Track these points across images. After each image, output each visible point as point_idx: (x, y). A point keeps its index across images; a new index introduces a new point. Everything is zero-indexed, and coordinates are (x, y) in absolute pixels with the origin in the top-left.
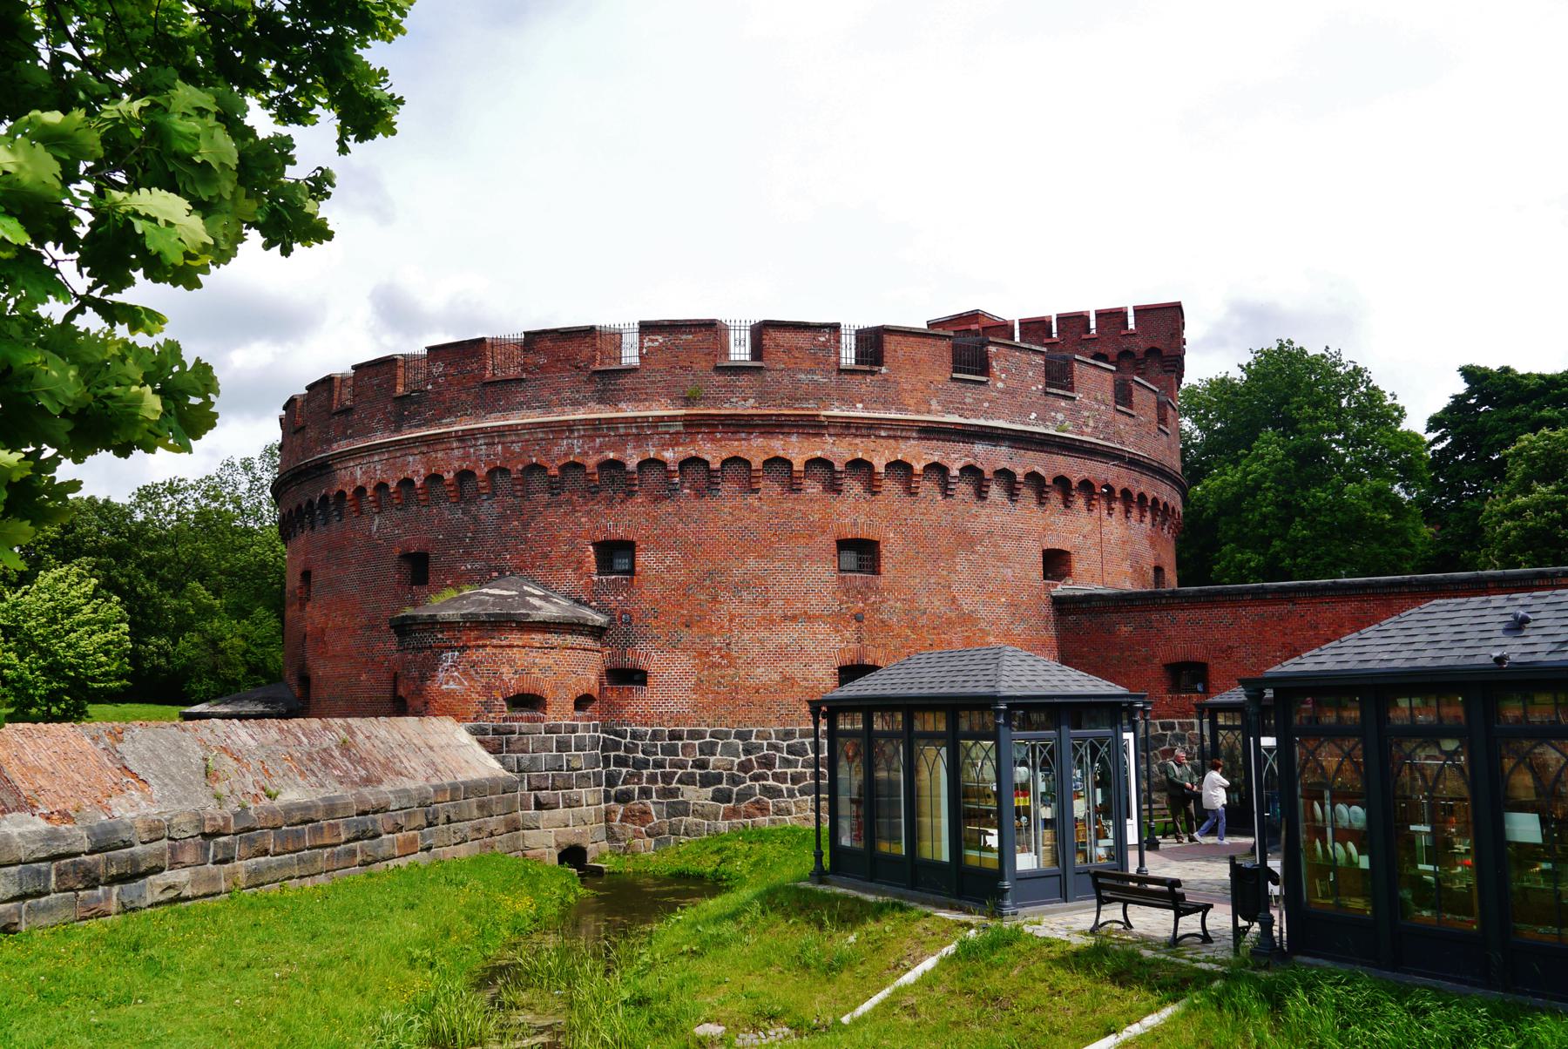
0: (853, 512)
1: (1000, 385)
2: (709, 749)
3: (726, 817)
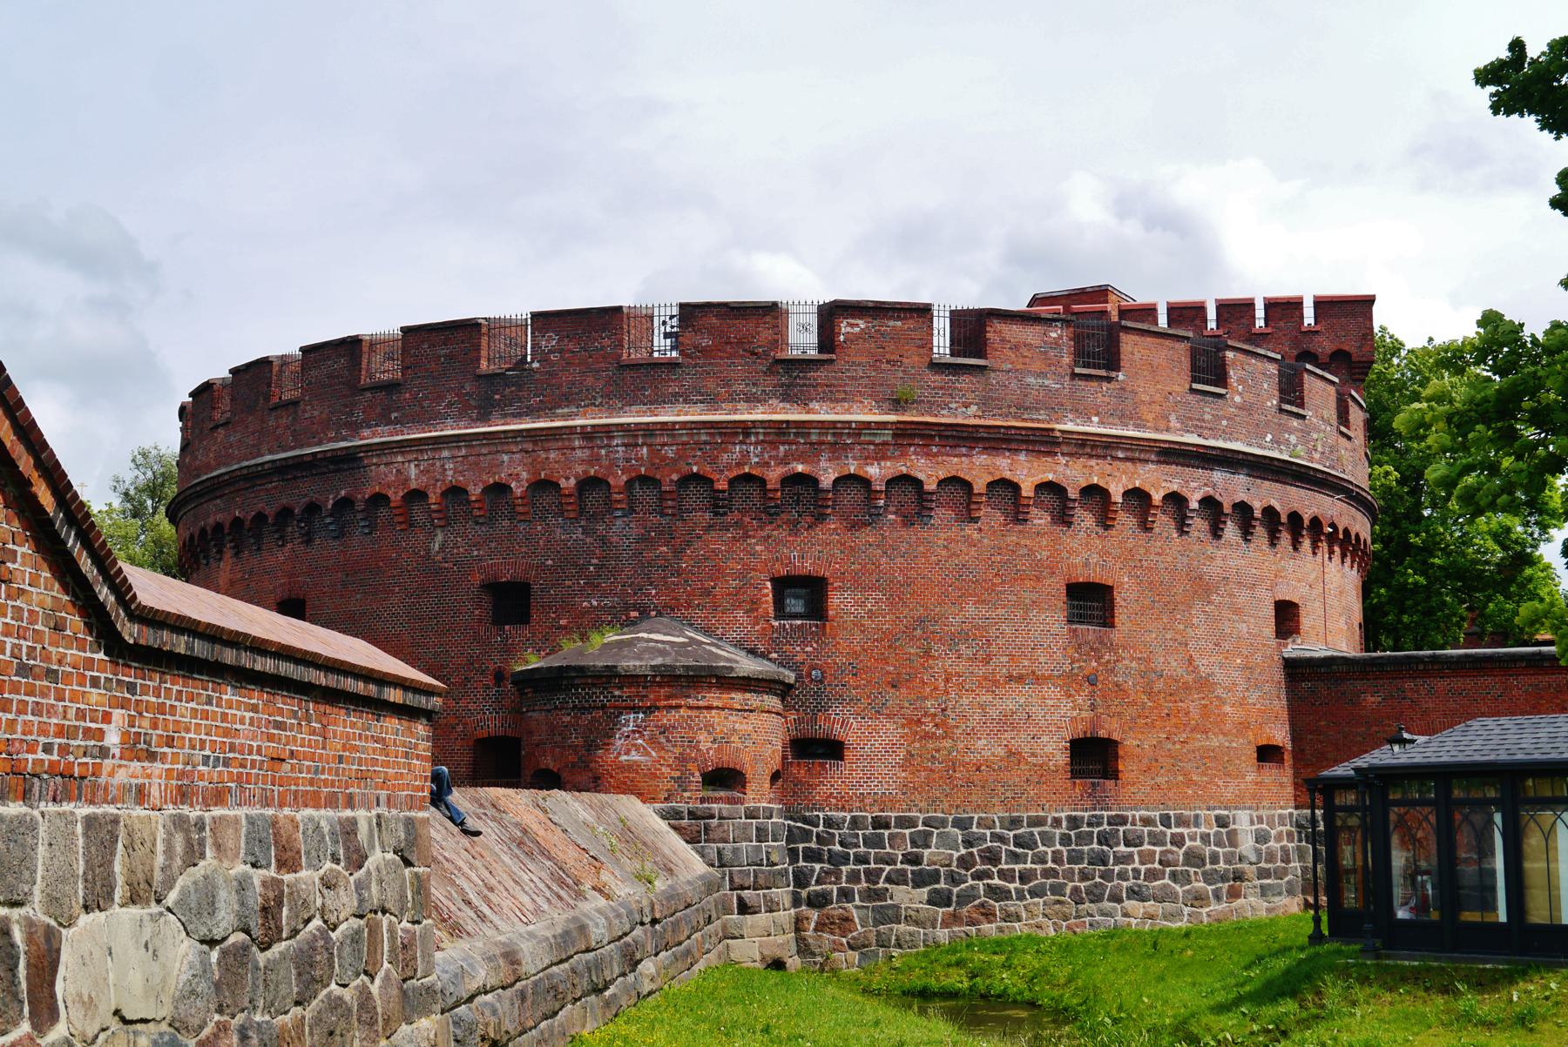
0: (1085, 550)
1: (1238, 399)
2: (922, 840)
3: (945, 924)
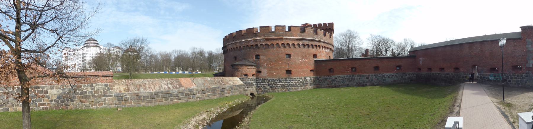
0: (288, 50)
2: (269, 81)
